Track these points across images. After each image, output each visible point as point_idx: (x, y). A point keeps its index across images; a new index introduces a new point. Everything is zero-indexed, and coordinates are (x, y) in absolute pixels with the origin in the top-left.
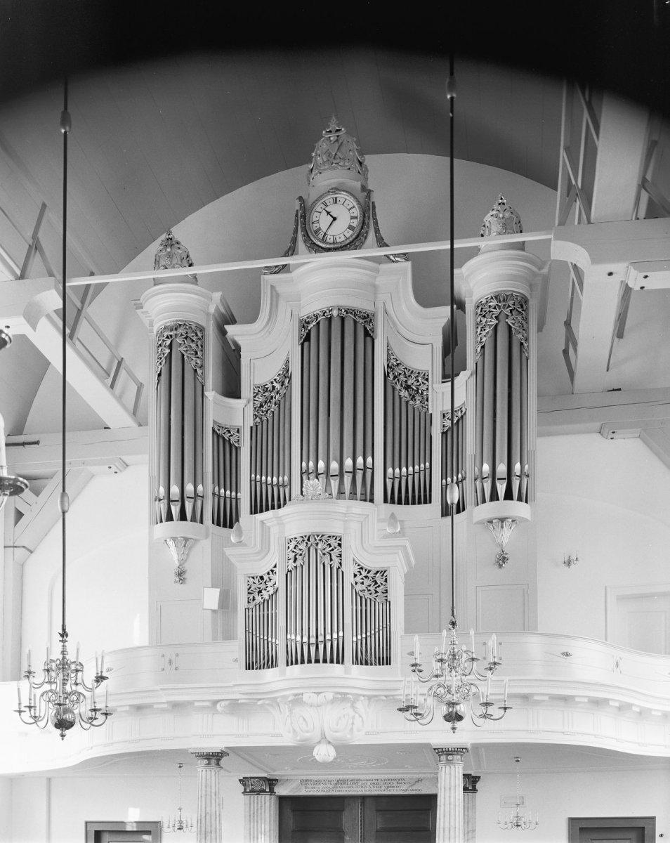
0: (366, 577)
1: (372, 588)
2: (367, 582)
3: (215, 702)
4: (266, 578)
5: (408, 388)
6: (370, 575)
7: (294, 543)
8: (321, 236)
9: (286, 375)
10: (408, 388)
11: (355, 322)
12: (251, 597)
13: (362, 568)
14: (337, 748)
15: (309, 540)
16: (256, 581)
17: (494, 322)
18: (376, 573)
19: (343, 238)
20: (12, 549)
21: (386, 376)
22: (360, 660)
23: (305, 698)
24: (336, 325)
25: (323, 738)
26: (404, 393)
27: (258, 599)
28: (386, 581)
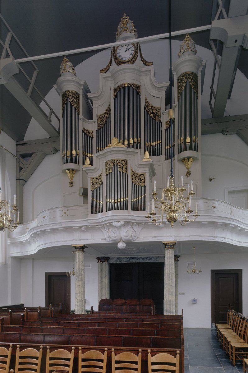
0: (136, 177)
1: (139, 181)
2: (137, 179)
3: (81, 227)
4: (98, 178)
5: (153, 113)
6: (138, 176)
7: (109, 163)
8: (120, 58)
9: (109, 110)
10: (153, 113)
11: (133, 89)
12: (93, 186)
13: (135, 173)
14: (126, 243)
15: (114, 162)
16: (95, 180)
17: (185, 84)
18: (140, 175)
19: (129, 58)
20: (19, 180)
21: (145, 109)
22: (135, 208)
23: (113, 224)
24: (127, 89)
25: (121, 240)
26: (152, 115)
27: (96, 187)
28: (144, 178)
